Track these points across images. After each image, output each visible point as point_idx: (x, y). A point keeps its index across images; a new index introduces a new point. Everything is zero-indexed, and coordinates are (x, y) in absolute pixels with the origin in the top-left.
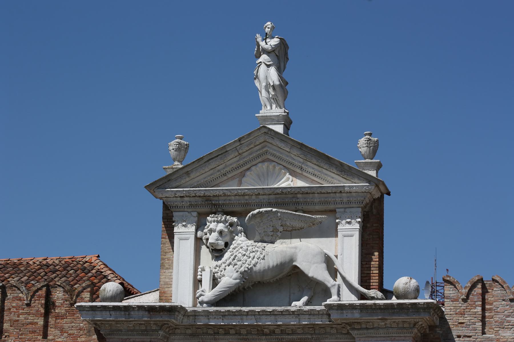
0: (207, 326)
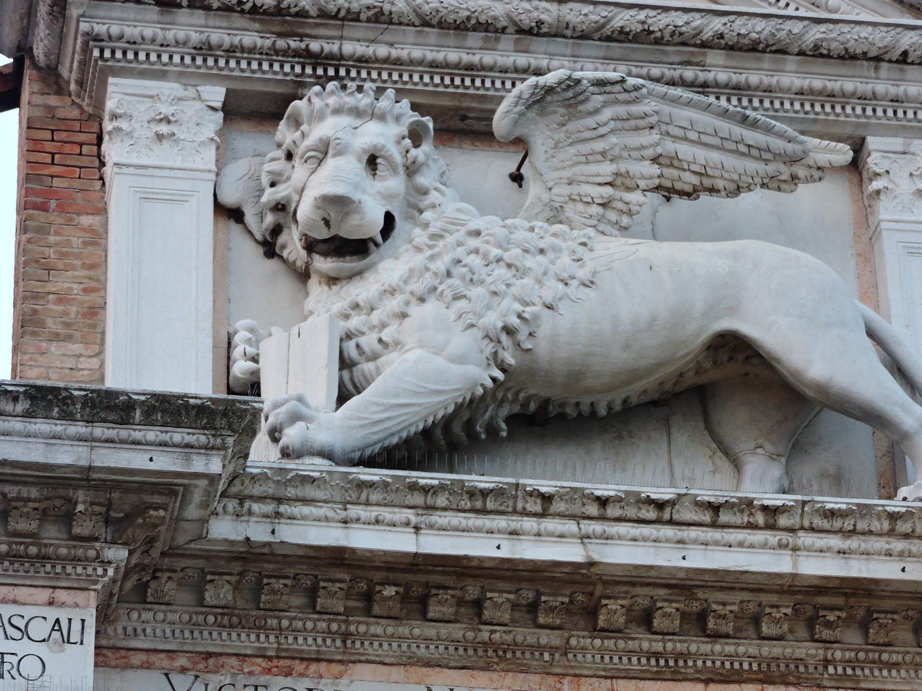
0: (339, 557)
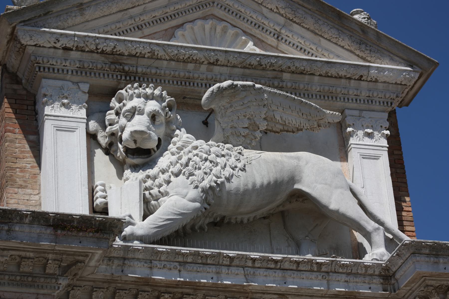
0: (146, 282)
